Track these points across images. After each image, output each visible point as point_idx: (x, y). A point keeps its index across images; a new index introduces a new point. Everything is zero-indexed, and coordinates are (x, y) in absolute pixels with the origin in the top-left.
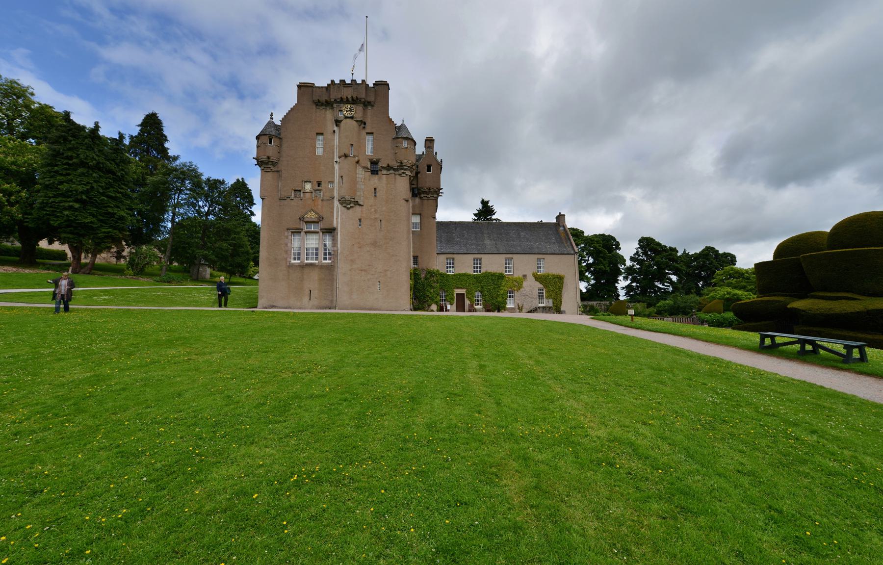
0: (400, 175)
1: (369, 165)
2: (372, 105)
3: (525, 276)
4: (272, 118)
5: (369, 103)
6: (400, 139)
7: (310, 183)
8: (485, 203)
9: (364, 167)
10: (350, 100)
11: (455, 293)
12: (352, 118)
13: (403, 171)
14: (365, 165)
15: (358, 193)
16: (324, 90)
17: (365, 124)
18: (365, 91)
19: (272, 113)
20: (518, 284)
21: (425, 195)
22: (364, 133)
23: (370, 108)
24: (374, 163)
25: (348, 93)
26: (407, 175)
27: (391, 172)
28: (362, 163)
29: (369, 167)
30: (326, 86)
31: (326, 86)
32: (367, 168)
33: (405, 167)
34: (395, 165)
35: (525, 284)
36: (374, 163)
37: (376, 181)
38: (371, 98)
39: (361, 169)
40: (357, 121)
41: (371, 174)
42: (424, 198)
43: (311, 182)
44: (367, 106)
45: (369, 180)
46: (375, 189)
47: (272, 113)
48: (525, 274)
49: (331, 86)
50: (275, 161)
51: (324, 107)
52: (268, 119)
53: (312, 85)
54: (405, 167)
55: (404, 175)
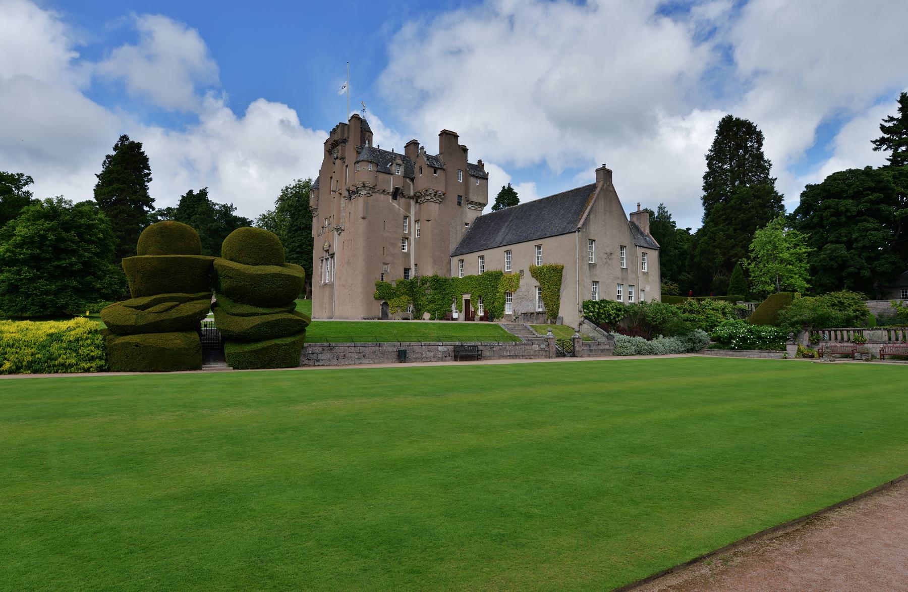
1: (346, 194)
3: (522, 271)
9: (345, 197)
11: (463, 299)
15: (341, 220)
20: (513, 283)
28: (343, 195)
33: (359, 188)
34: (353, 188)
35: (522, 282)
40: (340, 159)
48: (521, 269)
54: (359, 188)
55: (361, 196)
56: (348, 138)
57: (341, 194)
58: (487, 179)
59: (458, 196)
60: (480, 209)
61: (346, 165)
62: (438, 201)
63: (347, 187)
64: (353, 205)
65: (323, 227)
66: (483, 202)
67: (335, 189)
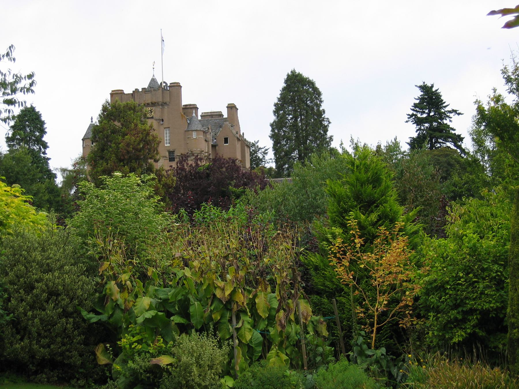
1: (167, 154)
2: (168, 105)
4: (92, 121)
5: (165, 103)
6: (190, 132)
8: (426, 89)
10: (150, 104)
14: (164, 155)
16: (131, 96)
17: (163, 120)
18: (161, 94)
19: (92, 117)
22: (162, 128)
23: (166, 107)
25: (148, 99)
29: (168, 157)
30: (132, 92)
31: (132, 92)
32: (166, 157)
38: (167, 100)
40: (156, 120)
41: (170, 161)
44: (163, 106)
47: (92, 117)
49: (136, 94)
52: (90, 123)
53: (121, 92)
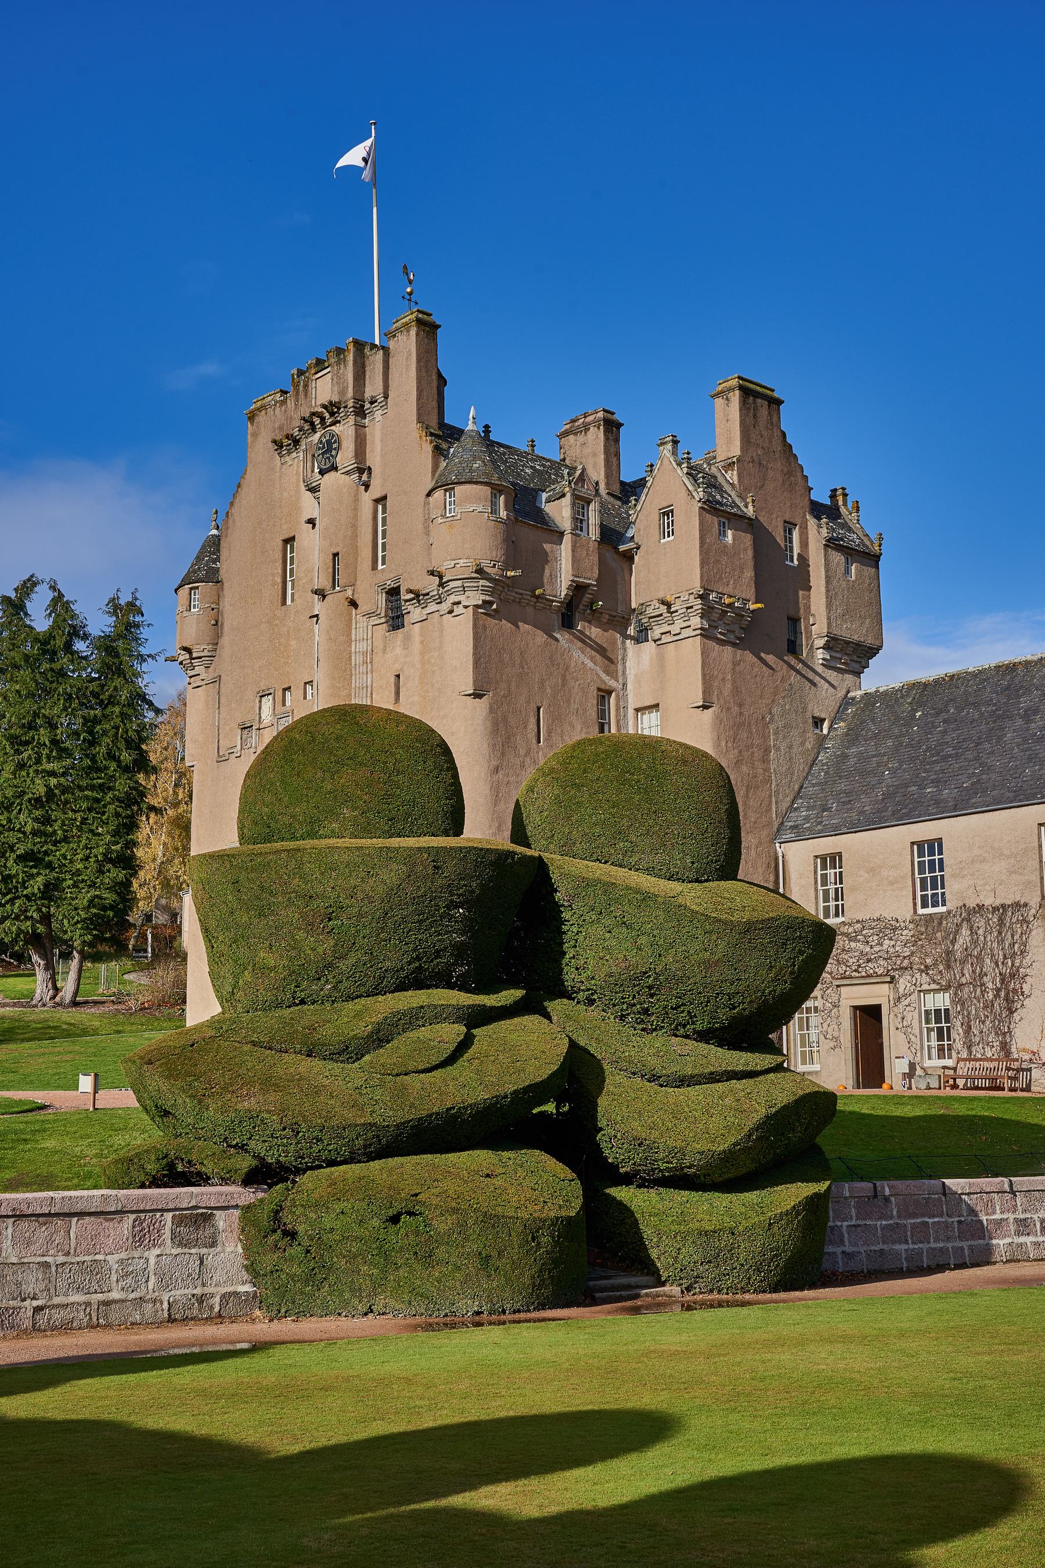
0: (451, 612)
7: (270, 697)
9: (369, 615)
10: (327, 415)
12: (333, 468)
13: (453, 598)
21: (666, 628)
24: (393, 593)
26: (466, 607)
27: (428, 610)
28: (363, 607)
33: (452, 584)
36: (393, 593)
37: (399, 651)
39: (362, 621)
40: (347, 473)
42: (665, 639)
43: (270, 694)
45: (384, 651)
46: (398, 676)
50: (206, 653)
51: (294, 455)
55: (459, 609)
56: (386, 397)
57: (353, 604)
58: (873, 559)
59: (788, 618)
60: (856, 666)
61: (375, 492)
62: (732, 637)
63: (386, 574)
64: (416, 646)
65: (245, 728)
66: (870, 641)
67: (324, 582)
